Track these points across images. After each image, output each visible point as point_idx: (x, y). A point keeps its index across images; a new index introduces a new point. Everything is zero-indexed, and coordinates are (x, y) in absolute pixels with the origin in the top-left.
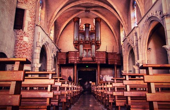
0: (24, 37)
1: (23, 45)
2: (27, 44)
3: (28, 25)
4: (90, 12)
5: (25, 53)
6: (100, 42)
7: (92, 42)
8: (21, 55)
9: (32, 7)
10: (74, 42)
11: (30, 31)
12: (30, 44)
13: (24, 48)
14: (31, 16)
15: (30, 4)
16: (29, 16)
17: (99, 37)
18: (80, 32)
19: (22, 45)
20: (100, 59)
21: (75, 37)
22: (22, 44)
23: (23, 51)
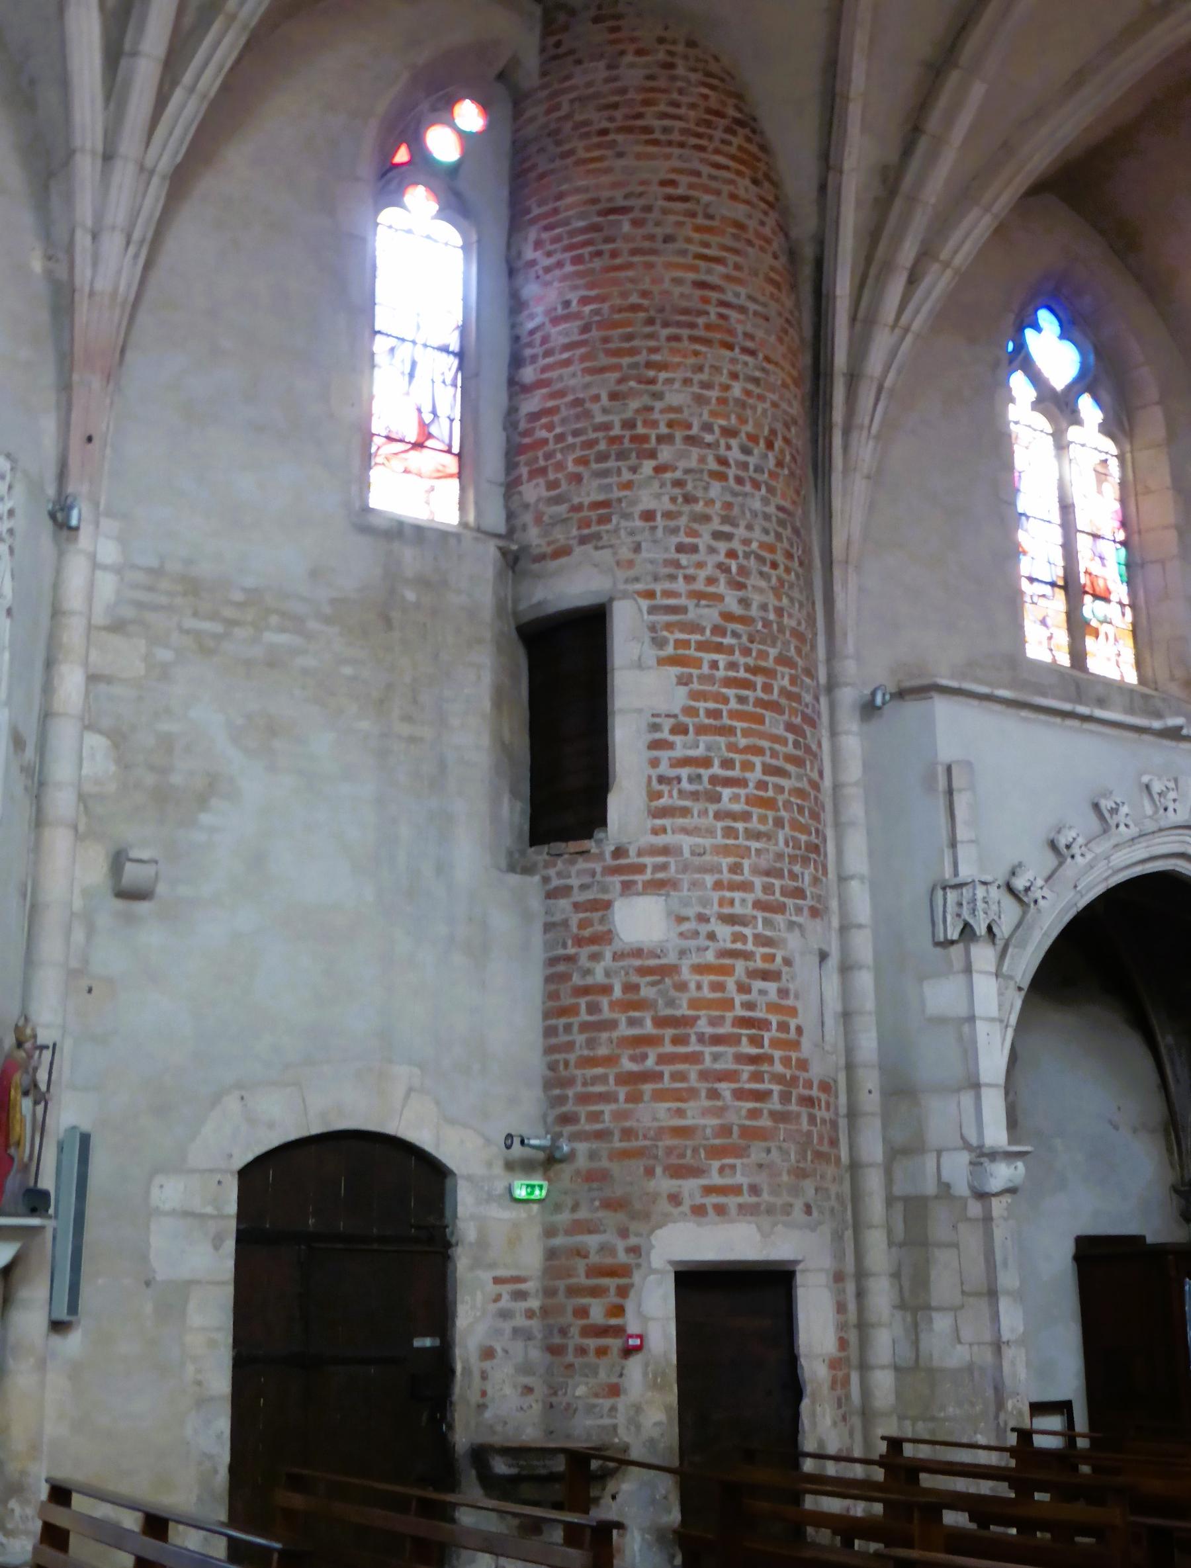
0: (617, 905)
1: (617, 992)
2: (671, 970)
3: (655, 763)
5: (657, 1076)
8: (607, 1109)
9: (674, 540)
11: (685, 812)
12: (710, 957)
13: (632, 1022)
14: (670, 650)
15: (648, 516)
16: (651, 654)
19: (605, 1002)
22: (606, 990)
23: (628, 1065)
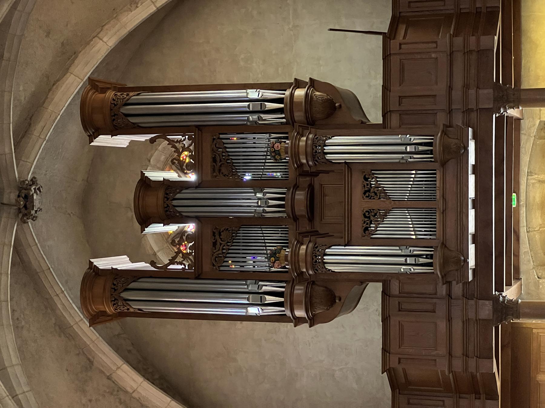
4: (34, 181)
6: (300, 93)
7: (295, 155)
10: (298, 321)
17: (253, 94)
18: (207, 267)
20: (450, 88)
21: (253, 311)
